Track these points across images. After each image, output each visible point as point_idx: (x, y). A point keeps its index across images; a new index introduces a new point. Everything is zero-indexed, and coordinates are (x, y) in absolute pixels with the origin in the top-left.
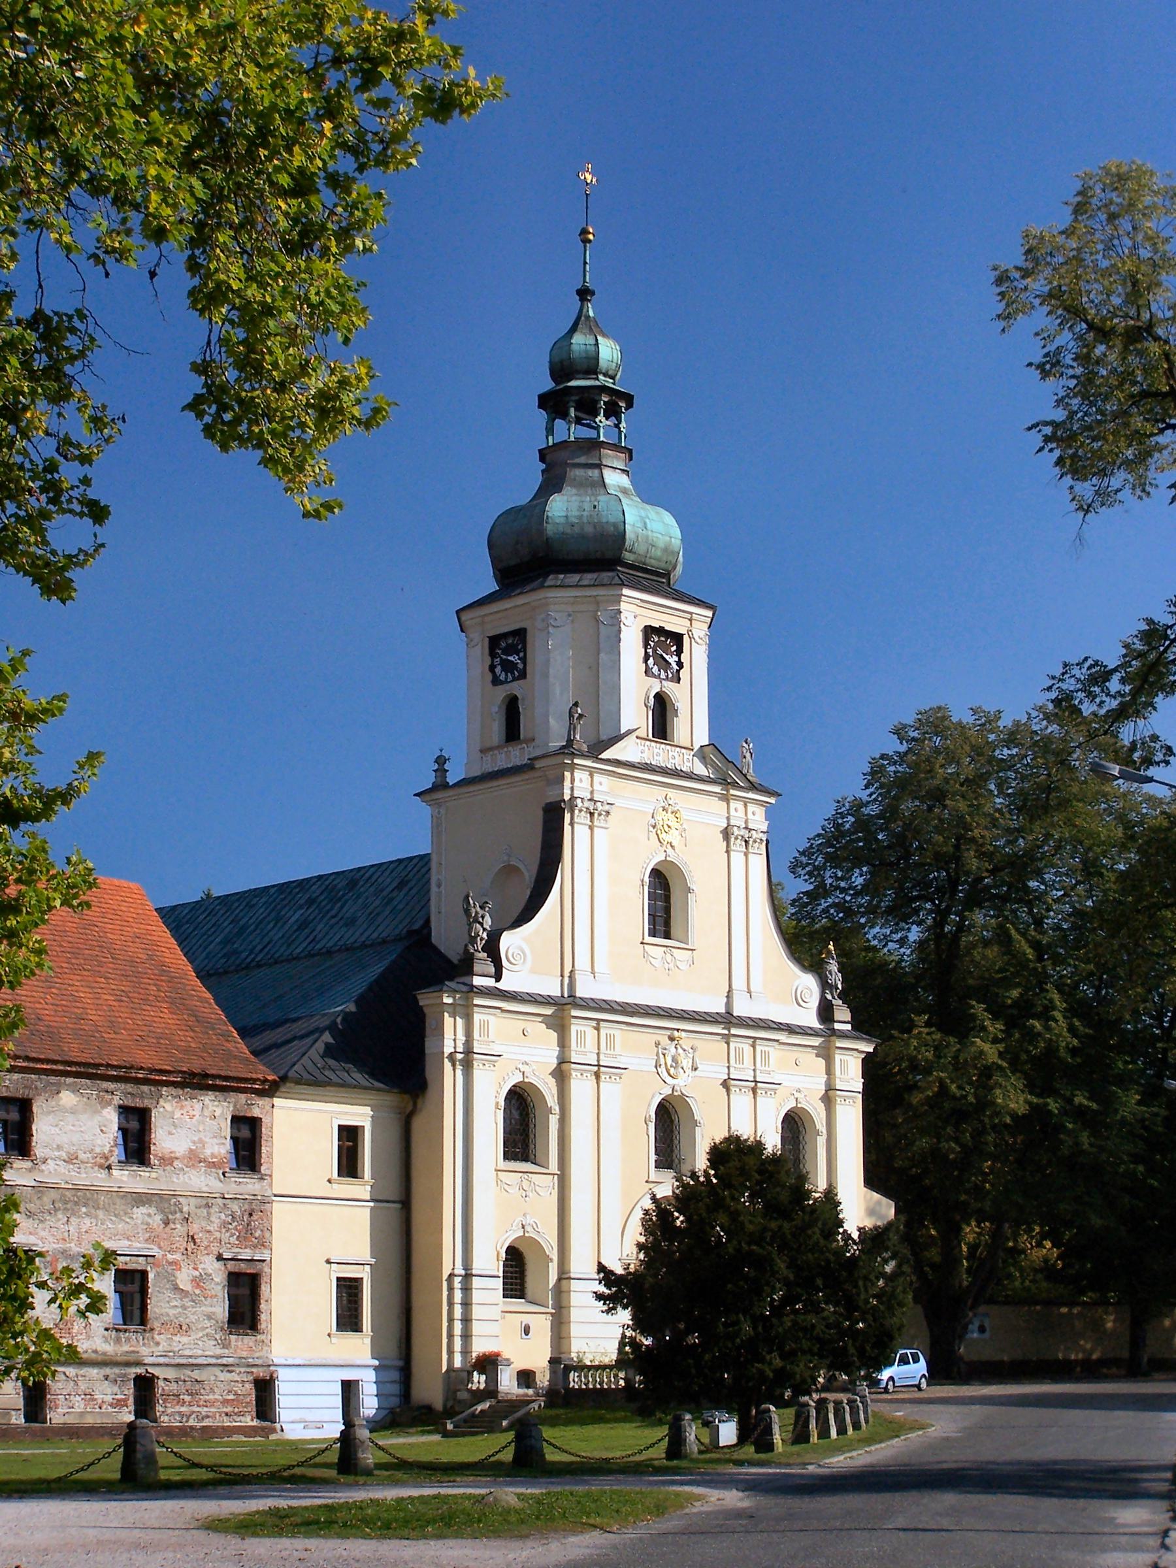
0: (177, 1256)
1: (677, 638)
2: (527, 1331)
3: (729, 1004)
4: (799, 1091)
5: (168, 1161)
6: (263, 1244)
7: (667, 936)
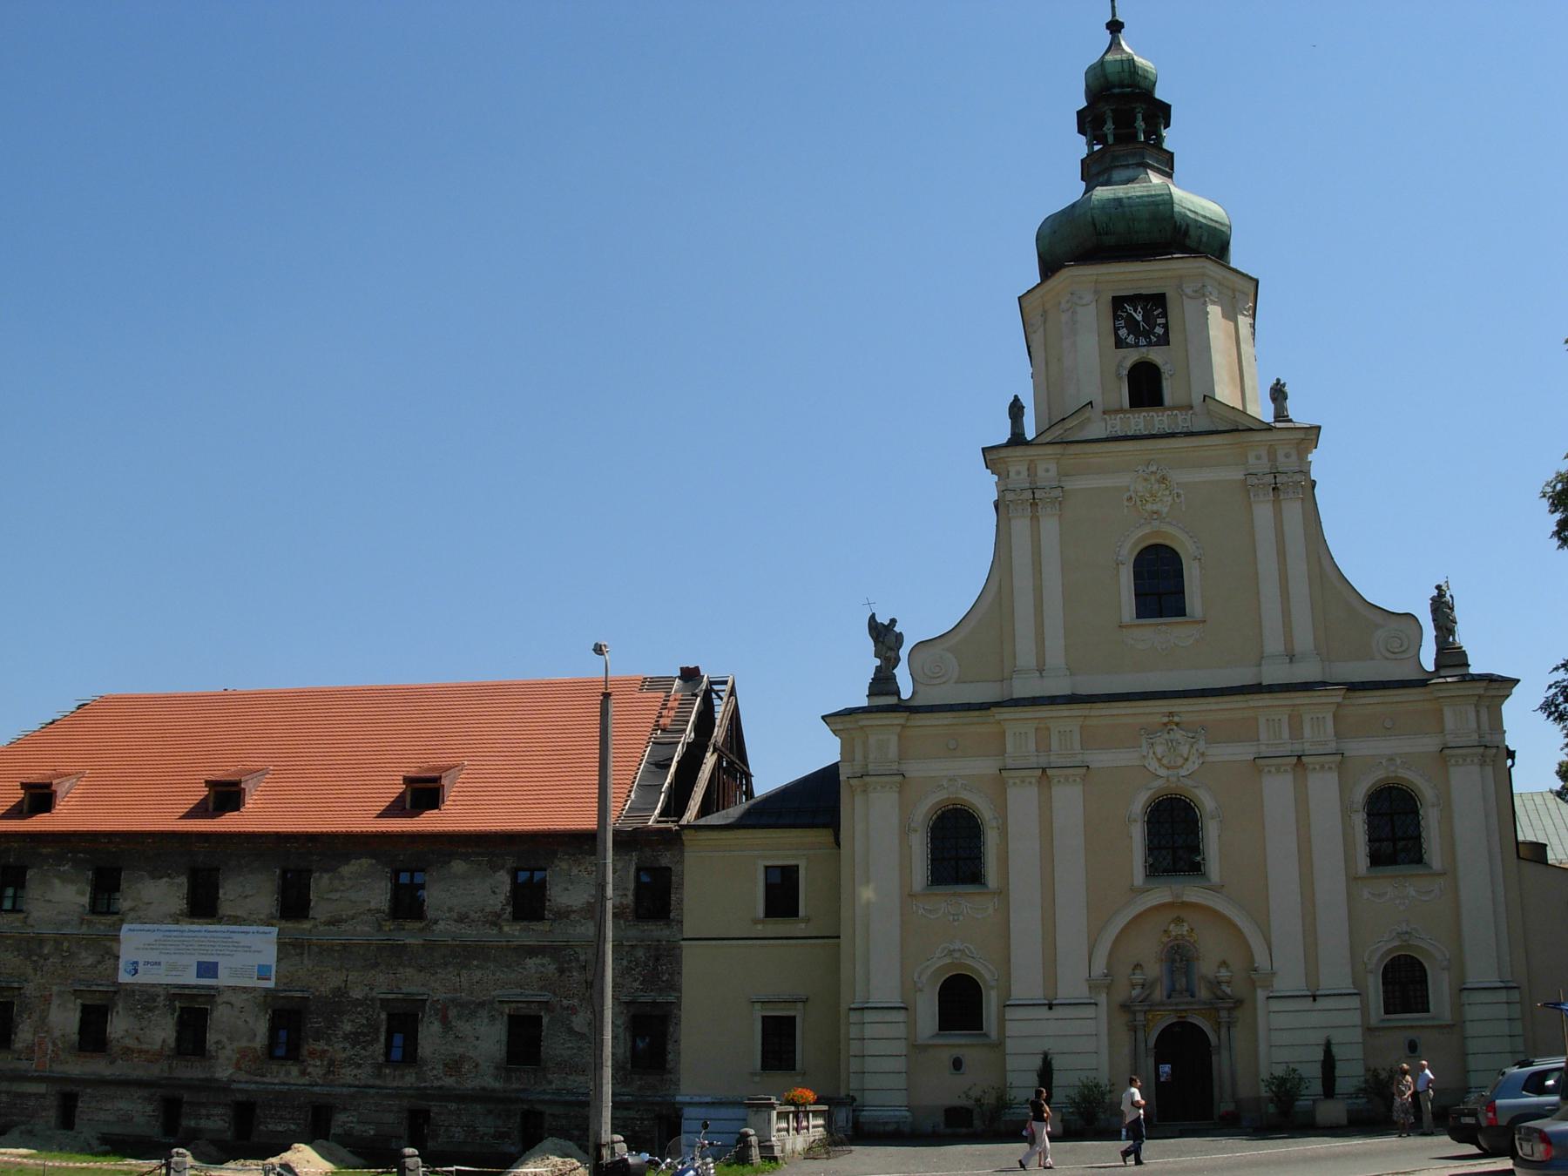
0: (575, 1002)
1: (1159, 300)
2: (957, 1064)
5: (563, 914)
6: (674, 986)
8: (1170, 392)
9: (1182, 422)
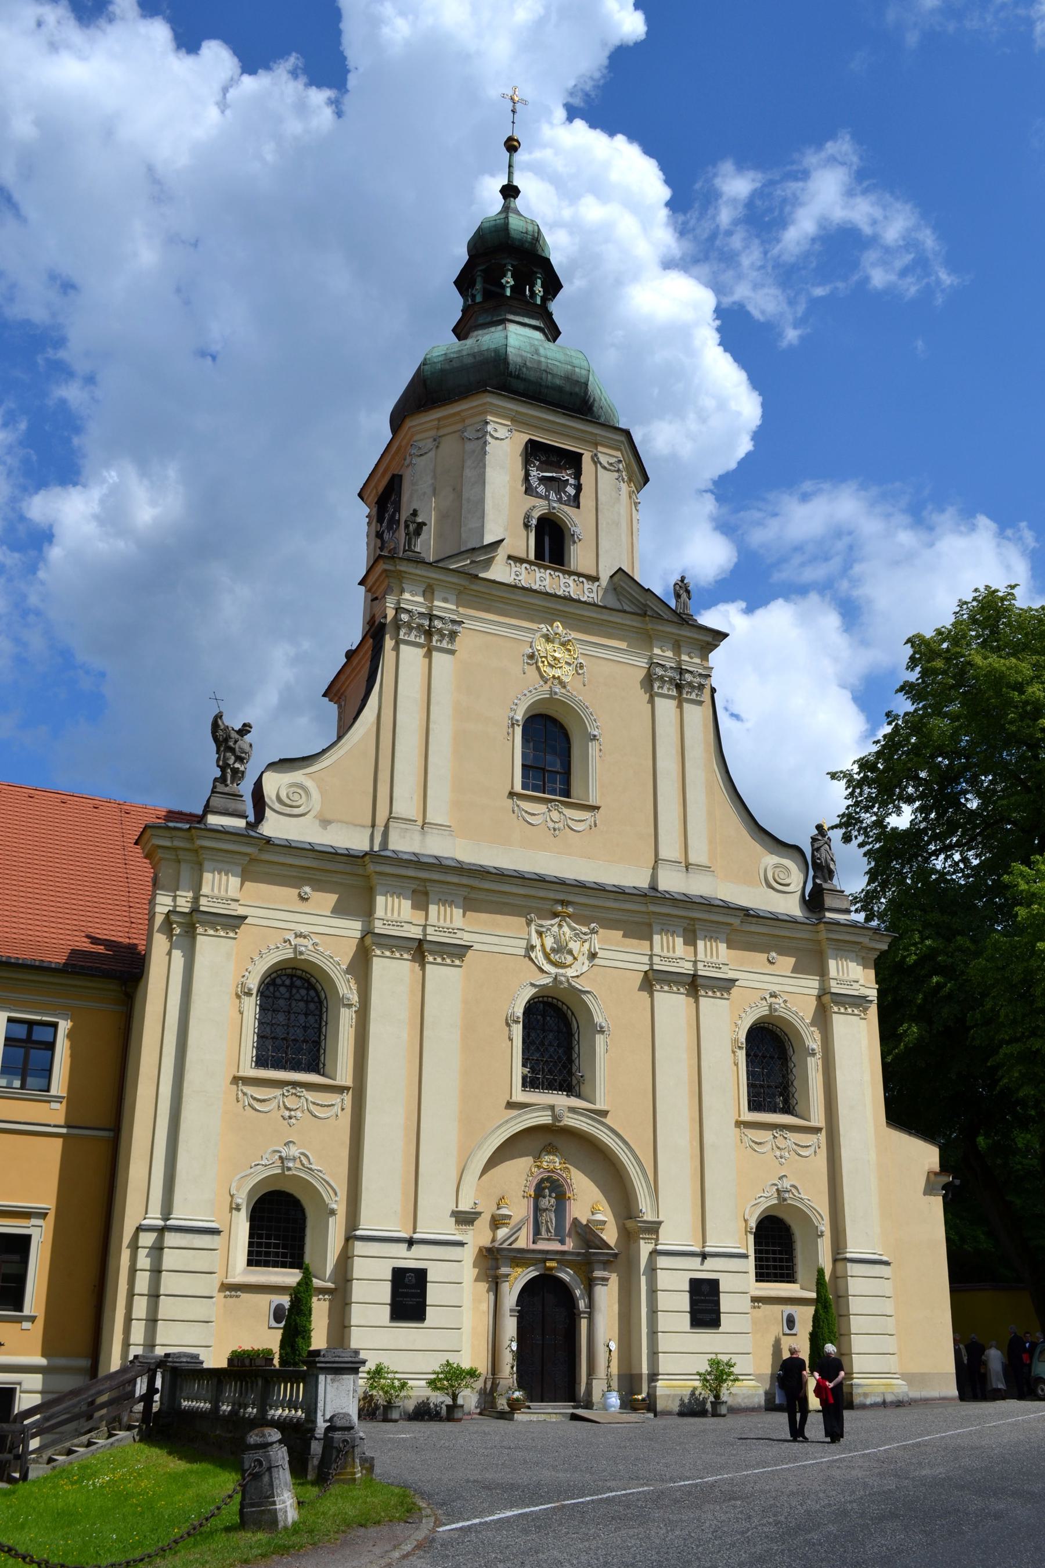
3: (654, 877)
4: (773, 995)
7: (568, 796)
8: (580, 557)
9: (587, 592)
